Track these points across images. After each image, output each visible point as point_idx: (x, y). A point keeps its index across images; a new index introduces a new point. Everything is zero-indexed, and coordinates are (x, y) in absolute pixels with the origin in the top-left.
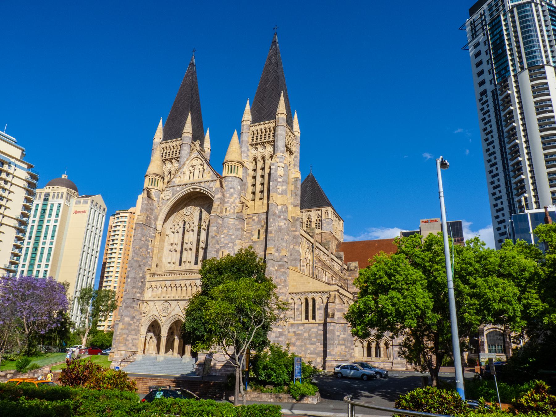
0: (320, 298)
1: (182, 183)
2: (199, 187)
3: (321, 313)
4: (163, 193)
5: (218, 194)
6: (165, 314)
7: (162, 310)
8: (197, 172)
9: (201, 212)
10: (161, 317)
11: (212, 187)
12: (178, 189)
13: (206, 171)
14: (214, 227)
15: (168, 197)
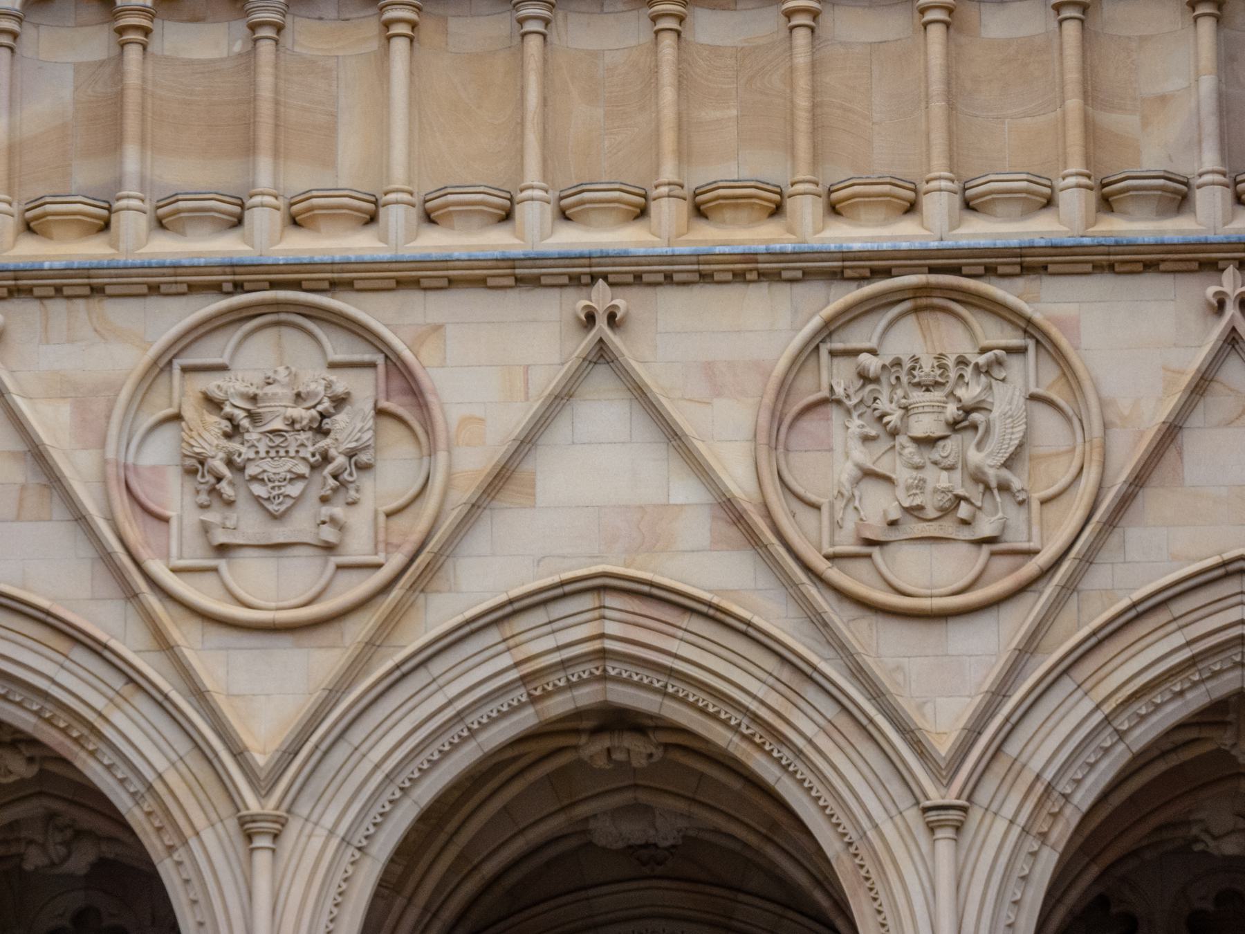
10: (184, 634)
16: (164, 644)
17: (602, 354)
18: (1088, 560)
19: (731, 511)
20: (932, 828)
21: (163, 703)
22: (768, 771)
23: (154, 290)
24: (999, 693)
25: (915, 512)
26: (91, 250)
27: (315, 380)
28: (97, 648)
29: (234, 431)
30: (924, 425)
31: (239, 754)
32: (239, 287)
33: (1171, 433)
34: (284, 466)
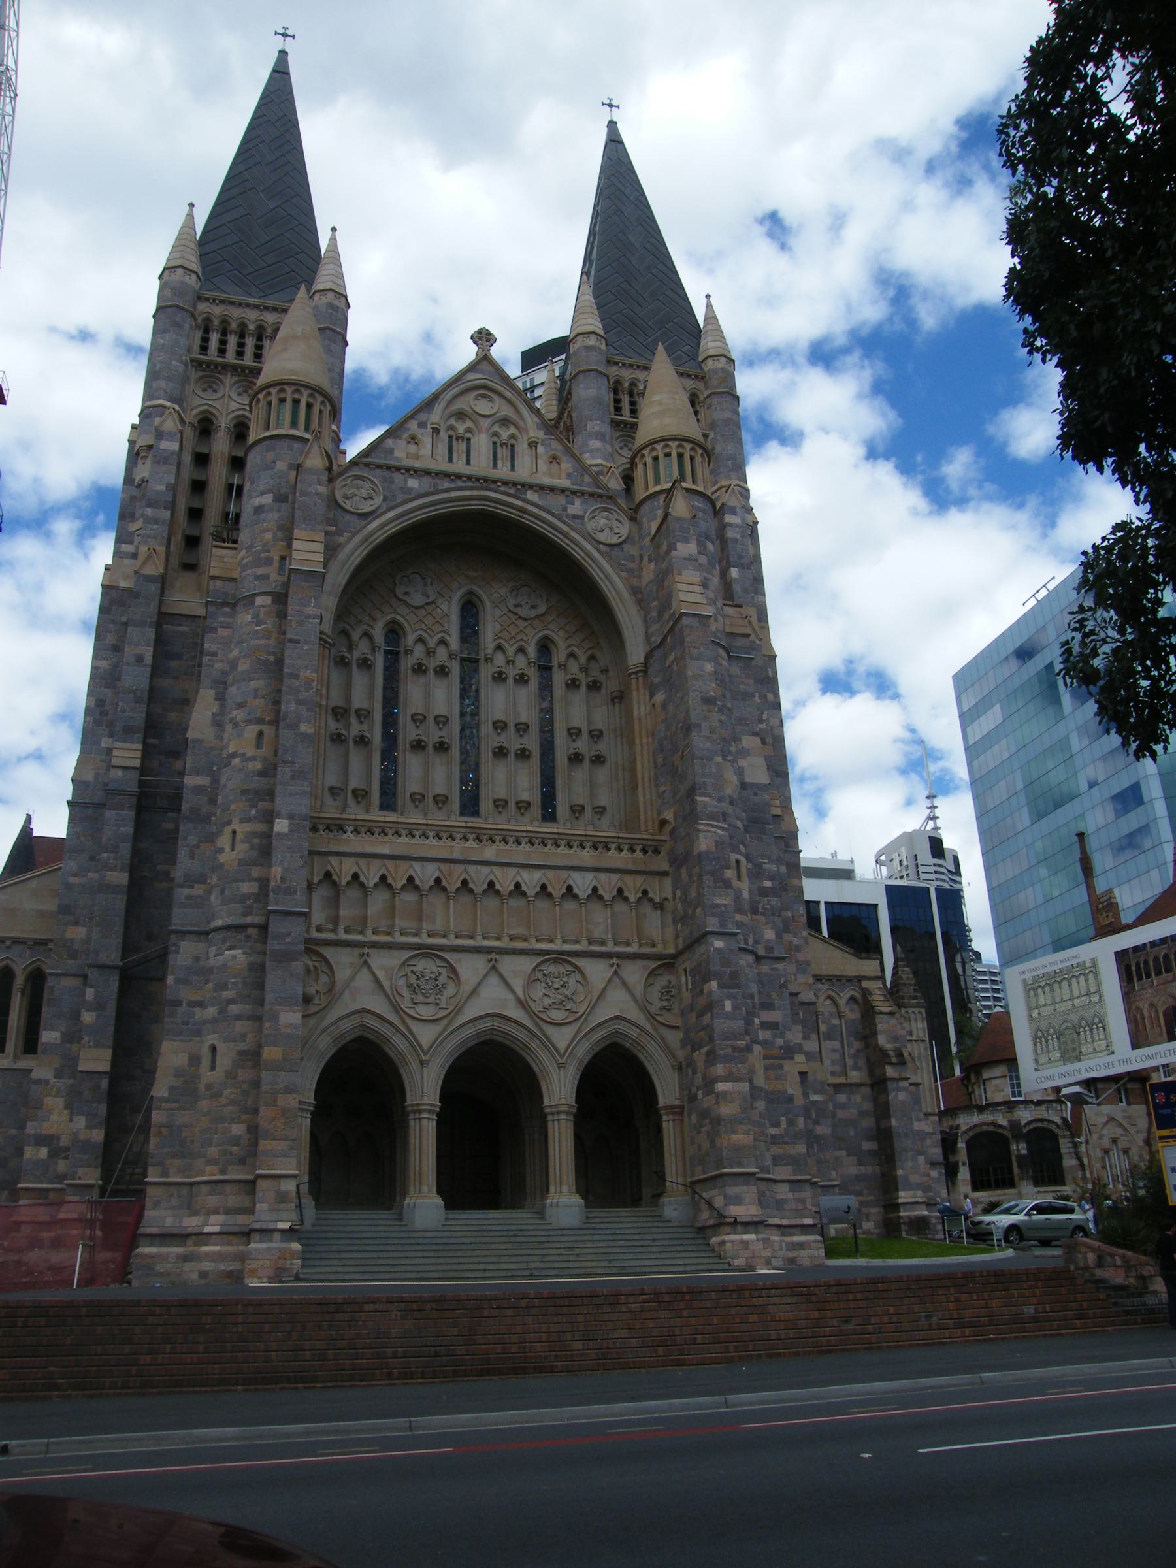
0: (829, 997)
1: (432, 466)
2: (519, 503)
3: (834, 1051)
4: (339, 483)
5: (686, 540)
6: (425, 1012)
7: (405, 992)
8: (482, 443)
9: (470, 610)
10: (409, 1021)
11: (581, 518)
12: (413, 483)
13: (540, 449)
14: (709, 661)
15: (366, 508)
16: (404, 1023)
17: (494, 967)
18: (589, 1014)
19: (519, 1001)
20: (559, 1067)
21: (404, 1035)
22: (524, 1055)
23: (402, 948)
24: (572, 1041)
25: (554, 1003)
26: (388, 939)
27: (435, 969)
28: (391, 1023)
29: (418, 979)
30: (556, 986)
31: (420, 1046)
32: (420, 949)
33: (604, 990)
34: (428, 987)
